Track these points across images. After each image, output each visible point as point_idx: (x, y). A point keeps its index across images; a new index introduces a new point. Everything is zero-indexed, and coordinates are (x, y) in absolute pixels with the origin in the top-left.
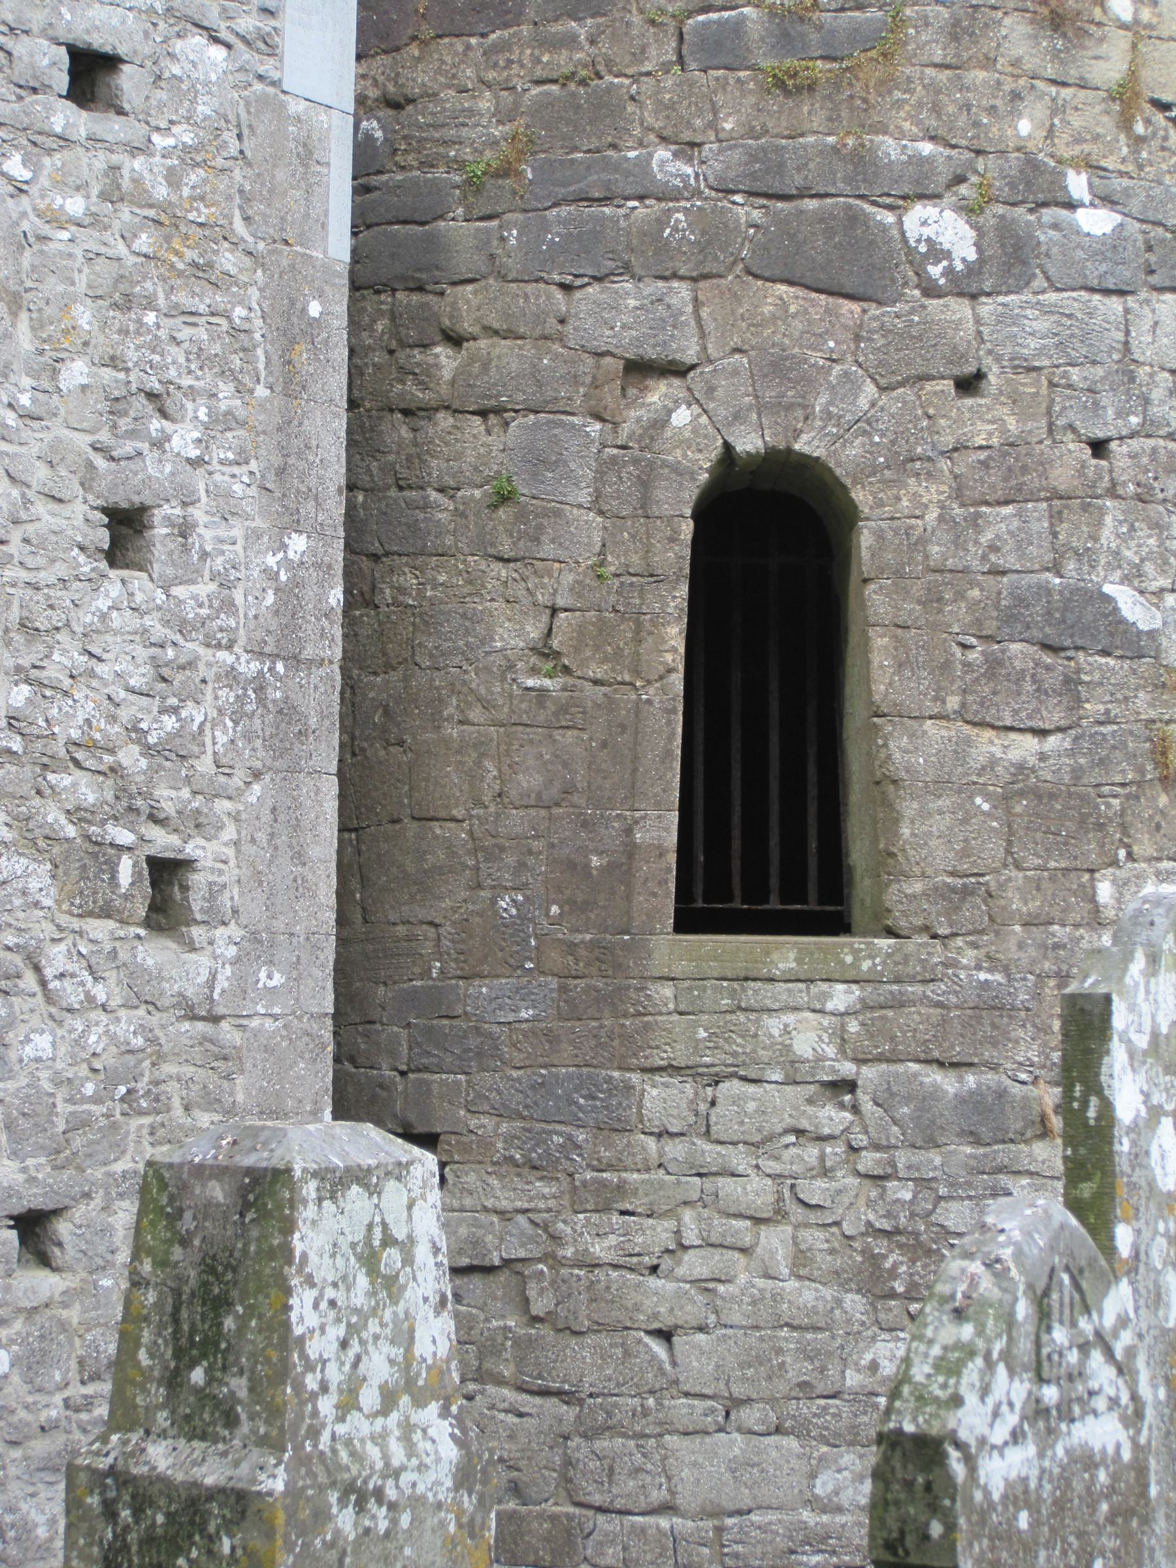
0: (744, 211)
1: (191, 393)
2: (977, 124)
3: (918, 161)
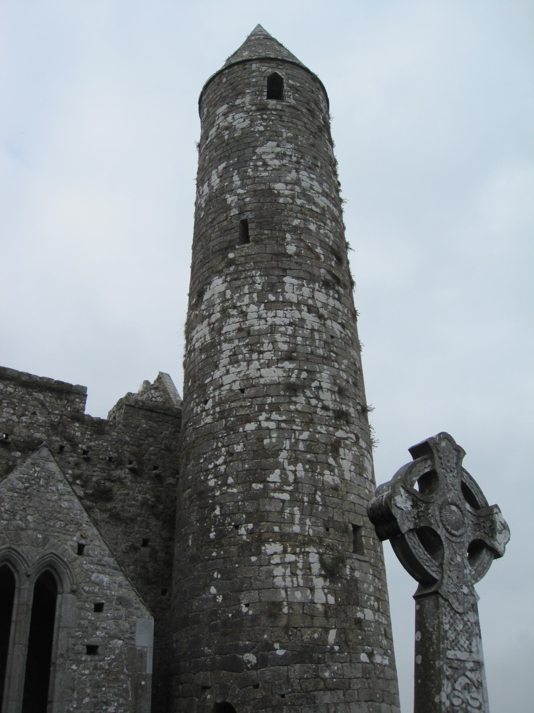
0: (218, 657)
1: (114, 701)
2: (256, 637)
3: (246, 645)
